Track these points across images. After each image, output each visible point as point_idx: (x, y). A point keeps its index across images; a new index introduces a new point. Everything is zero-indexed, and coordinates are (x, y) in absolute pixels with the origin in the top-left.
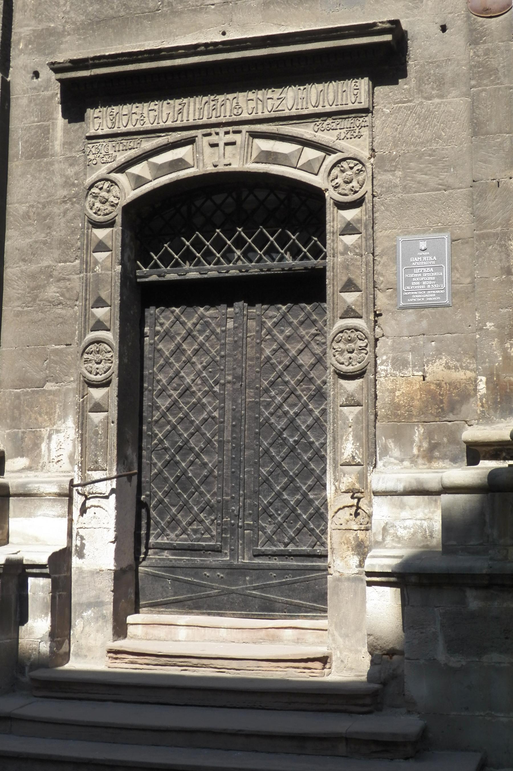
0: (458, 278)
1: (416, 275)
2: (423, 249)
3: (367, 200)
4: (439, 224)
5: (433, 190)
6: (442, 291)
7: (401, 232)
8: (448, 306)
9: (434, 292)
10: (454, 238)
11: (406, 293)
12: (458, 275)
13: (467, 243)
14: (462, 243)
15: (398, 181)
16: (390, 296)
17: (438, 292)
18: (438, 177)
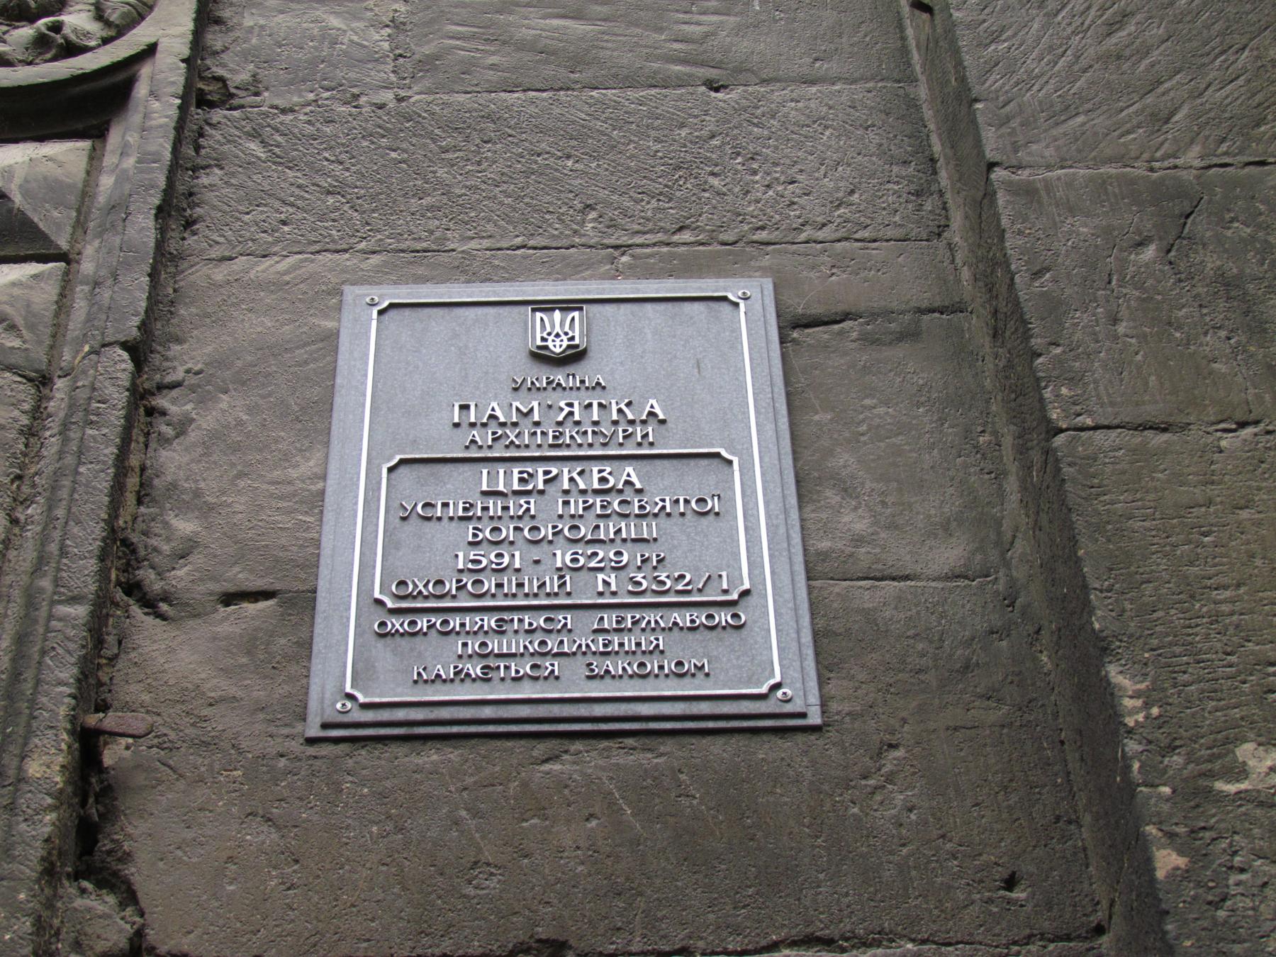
0: (858, 540)
1: (495, 506)
2: (557, 347)
3: (141, 90)
4: (686, 236)
5: (629, 82)
6: (723, 617)
7: (377, 269)
8: (786, 727)
9: (651, 616)
10: (799, 307)
11: (395, 623)
12: (856, 522)
13: (909, 335)
14: (869, 340)
15: (380, 39)
16: (250, 645)
17: (683, 618)
18: (660, 30)
